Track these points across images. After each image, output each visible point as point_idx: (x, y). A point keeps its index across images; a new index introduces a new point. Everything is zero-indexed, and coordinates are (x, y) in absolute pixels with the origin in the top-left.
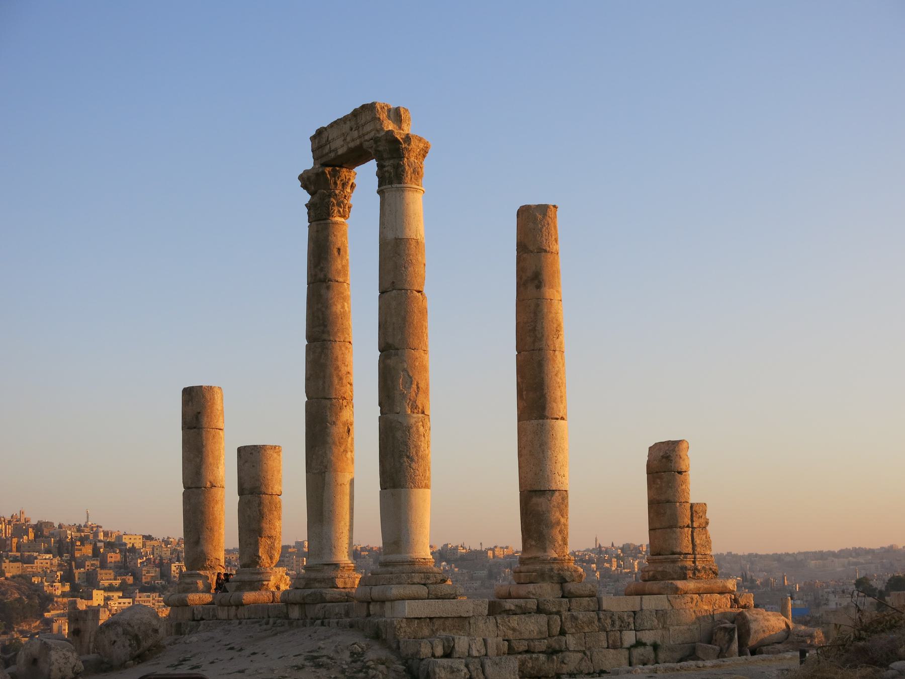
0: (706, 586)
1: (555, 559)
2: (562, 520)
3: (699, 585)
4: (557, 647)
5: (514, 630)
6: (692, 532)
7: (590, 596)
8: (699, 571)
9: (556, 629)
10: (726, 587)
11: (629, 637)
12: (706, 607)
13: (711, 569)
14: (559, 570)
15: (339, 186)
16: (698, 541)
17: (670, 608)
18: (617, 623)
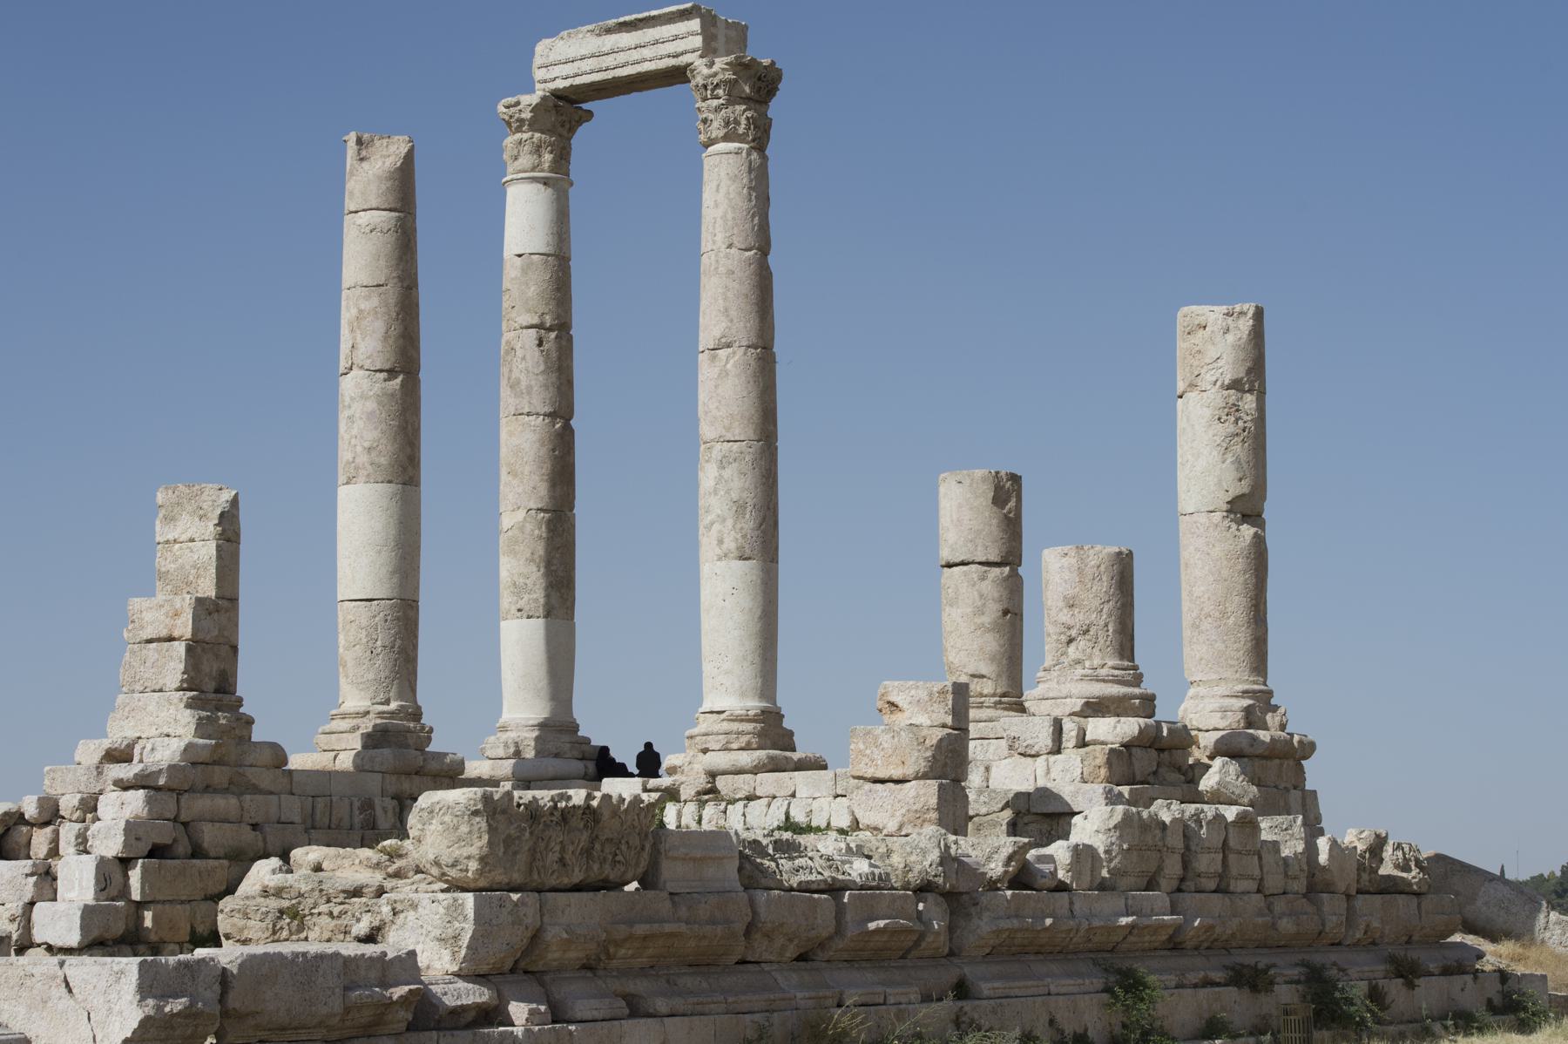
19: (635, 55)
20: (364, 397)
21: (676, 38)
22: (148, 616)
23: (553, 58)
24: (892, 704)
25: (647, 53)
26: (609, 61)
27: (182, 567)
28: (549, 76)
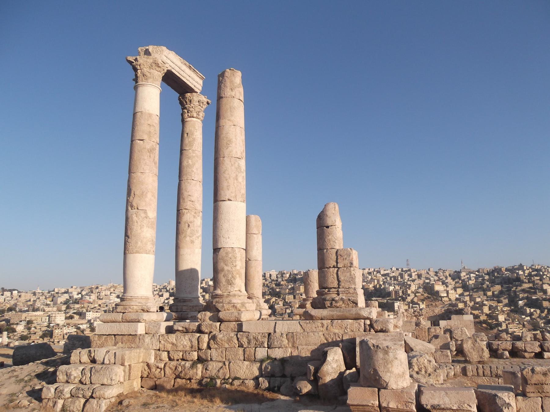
0: (339, 314)
1: (217, 295)
2: (226, 268)
3: (331, 313)
4: (204, 357)
5: (173, 344)
6: (337, 271)
7: (236, 321)
8: (336, 301)
9: (205, 346)
10: (359, 314)
11: (261, 353)
12: (336, 331)
13: (349, 300)
14: (217, 302)
15: (188, 103)
16: (342, 278)
17: (302, 331)
18: (253, 342)
19: (188, 78)
23: (169, 57)
26: (182, 73)
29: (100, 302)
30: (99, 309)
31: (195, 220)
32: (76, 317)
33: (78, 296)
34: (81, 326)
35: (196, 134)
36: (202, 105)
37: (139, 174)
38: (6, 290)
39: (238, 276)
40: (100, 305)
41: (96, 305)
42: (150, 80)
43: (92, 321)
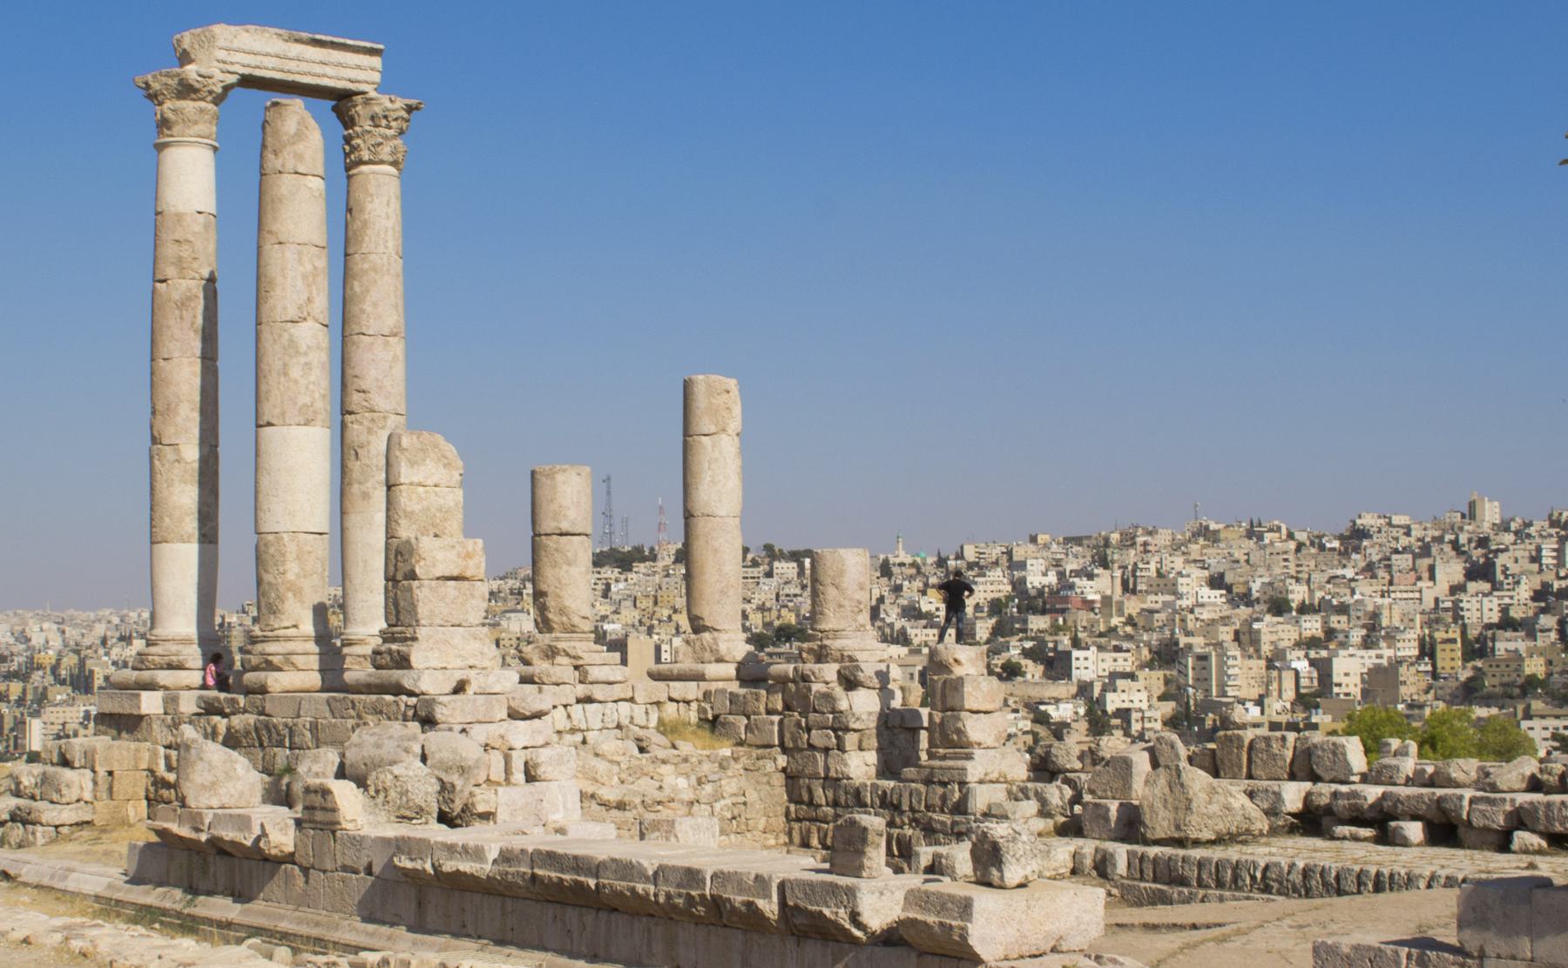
19: (318, 69)
20: (319, 347)
21: (359, 67)
22: (440, 556)
23: (236, 45)
24: (956, 660)
25: (329, 70)
26: (292, 65)
27: (428, 509)
28: (229, 59)
29: (1133, 606)
30: (1129, 637)
31: (372, 438)
32: (1033, 670)
33: (1046, 581)
34: (1050, 709)
35: (369, 207)
36: (384, 122)
37: (162, 363)
38: (782, 556)
39: (290, 595)
40: (1130, 621)
41: (1116, 621)
42: (176, 129)
43: (1097, 692)
